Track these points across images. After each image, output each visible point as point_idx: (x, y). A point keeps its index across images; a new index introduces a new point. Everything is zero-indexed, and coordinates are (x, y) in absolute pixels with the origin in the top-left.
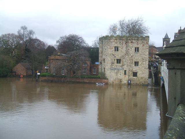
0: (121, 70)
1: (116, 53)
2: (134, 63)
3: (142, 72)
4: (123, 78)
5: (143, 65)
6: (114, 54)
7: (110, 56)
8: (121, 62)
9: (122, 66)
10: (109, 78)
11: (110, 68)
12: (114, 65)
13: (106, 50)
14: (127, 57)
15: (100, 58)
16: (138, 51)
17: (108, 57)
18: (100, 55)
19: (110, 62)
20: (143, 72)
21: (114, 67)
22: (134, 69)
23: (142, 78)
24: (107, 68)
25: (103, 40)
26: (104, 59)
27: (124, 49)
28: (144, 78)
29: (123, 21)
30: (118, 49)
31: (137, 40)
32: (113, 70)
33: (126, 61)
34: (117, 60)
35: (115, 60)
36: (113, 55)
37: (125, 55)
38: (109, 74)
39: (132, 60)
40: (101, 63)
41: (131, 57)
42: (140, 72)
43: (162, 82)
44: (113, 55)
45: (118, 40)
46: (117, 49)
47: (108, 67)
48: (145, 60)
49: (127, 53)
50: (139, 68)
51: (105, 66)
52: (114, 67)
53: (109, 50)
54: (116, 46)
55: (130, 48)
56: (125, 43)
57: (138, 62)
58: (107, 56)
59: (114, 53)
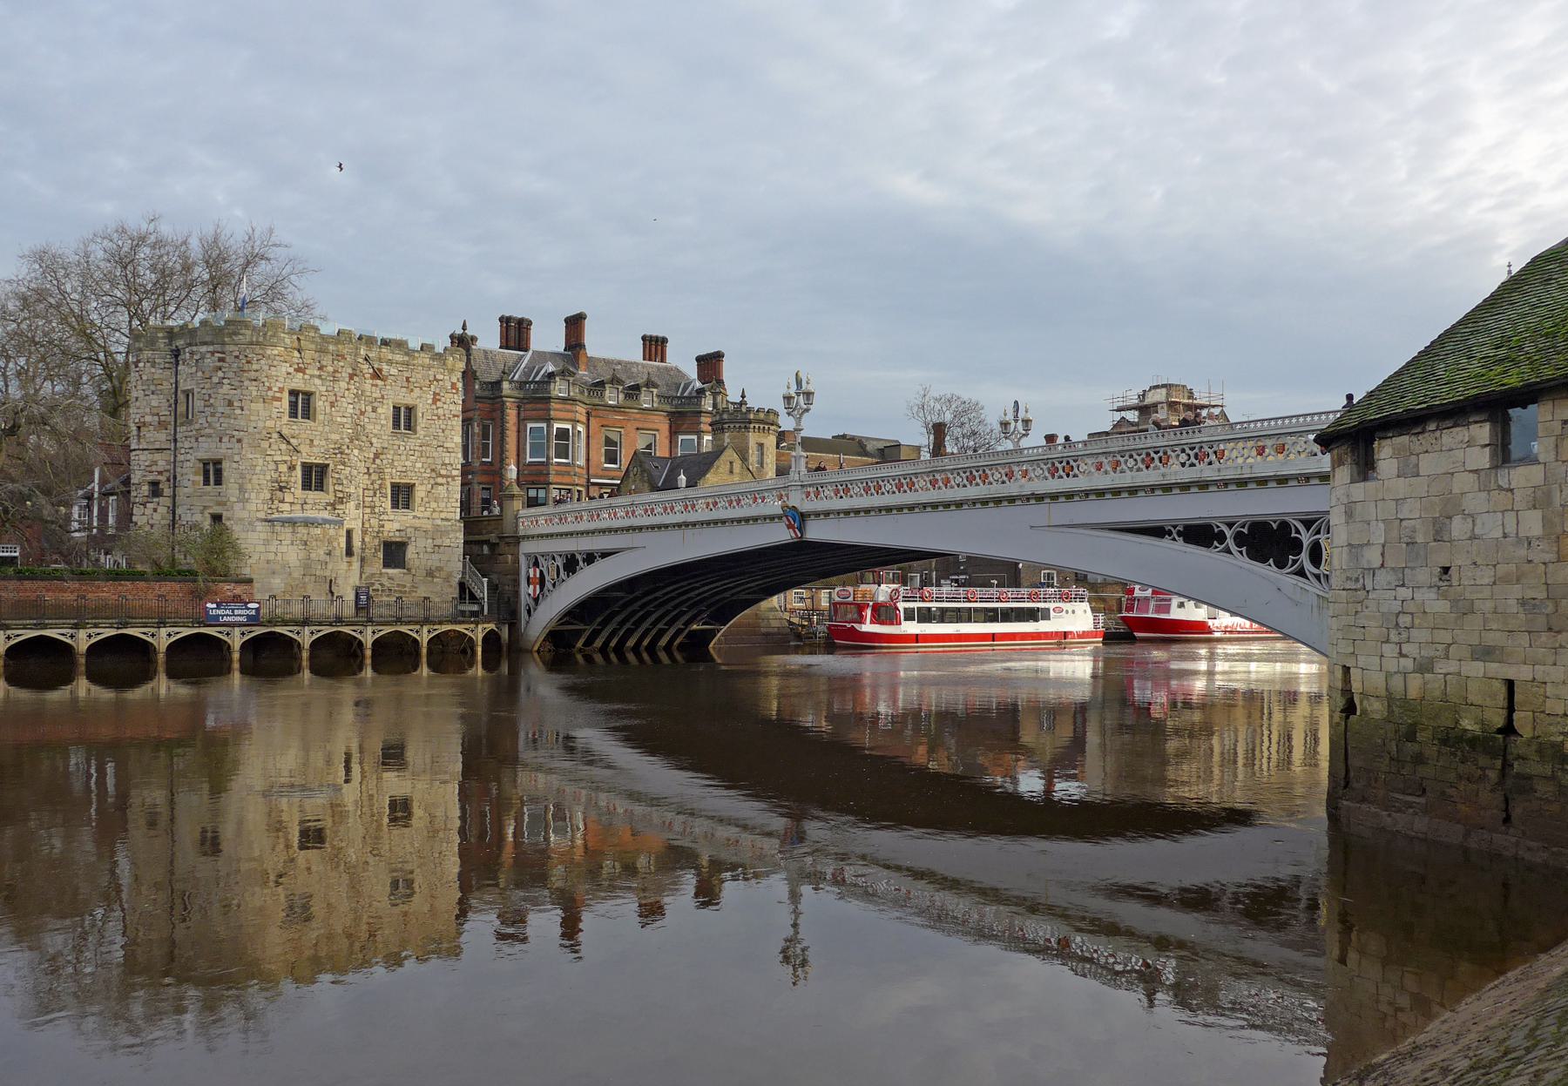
1: (300, 429)
5: (434, 505)
6: (285, 432)
7: (265, 444)
8: (330, 482)
9: (333, 505)
11: (262, 515)
13: (230, 404)
14: (356, 452)
16: (409, 427)
20: (438, 542)
21: (286, 507)
22: (388, 526)
23: (430, 574)
24: (245, 514)
25: (205, 343)
28: (443, 574)
29: (215, 241)
33: (353, 477)
34: (307, 469)
35: (292, 468)
38: (262, 549)
39: (380, 471)
41: (377, 456)
42: (421, 543)
46: (302, 404)
51: (223, 504)
55: (369, 408)
56: (351, 377)
57: (410, 488)
59: (285, 424)
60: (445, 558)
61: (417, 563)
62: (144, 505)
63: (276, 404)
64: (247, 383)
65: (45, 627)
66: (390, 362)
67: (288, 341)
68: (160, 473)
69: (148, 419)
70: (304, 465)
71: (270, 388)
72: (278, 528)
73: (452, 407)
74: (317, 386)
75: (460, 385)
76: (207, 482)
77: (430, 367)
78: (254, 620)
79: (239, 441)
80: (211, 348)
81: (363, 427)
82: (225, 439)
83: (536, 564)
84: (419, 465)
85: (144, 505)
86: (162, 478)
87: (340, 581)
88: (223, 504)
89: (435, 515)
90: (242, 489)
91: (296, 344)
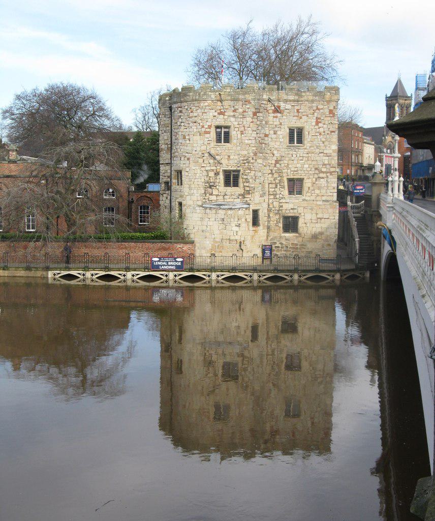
0: (239, 209)
2: (286, 184)
3: (314, 217)
5: (317, 191)
6: (213, 152)
7: (201, 161)
8: (241, 180)
9: (243, 196)
10: (196, 240)
12: (215, 192)
13: (184, 138)
14: (260, 161)
15: (162, 168)
16: (300, 141)
17: (193, 166)
18: (164, 157)
20: (320, 216)
21: (213, 198)
22: (285, 206)
23: (315, 237)
25: (175, 103)
26: (179, 173)
27: (251, 134)
28: (323, 237)
29: (244, 34)
30: (227, 135)
31: (294, 101)
34: (227, 174)
35: (217, 174)
36: (210, 155)
37: (255, 154)
38: (199, 223)
39: (280, 172)
40: (168, 186)
41: (277, 162)
43: (386, 249)
44: (210, 155)
45: (225, 103)
46: (223, 135)
47: (195, 198)
48: (326, 172)
49: (261, 147)
50: (304, 200)
51: (182, 196)
52: (213, 198)
53: (198, 137)
54: (222, 123)
55: (272, 132)
56: (255, 114)
57: (301, 181)
58: (188, 159)
59: (214, 147)
60: (325, 226)
61: (305, 229)
63: (207, 135)
64: (191, 124)
65: (69, 269)
66: (286, 101)
67: (213, 96)
68: (168, 177)
69: (163, 147)
71: (203, 127)
73: (331, 126)
74: (232, 122)
76: (178, 185)
77: (313, 101)
78: (179, 268)
82: (182, 159)
84: (306, 166)
86: (169, 180)
87: (248, 243)
89: (318, 198)
90: (190, 188)
91: (218, 98)
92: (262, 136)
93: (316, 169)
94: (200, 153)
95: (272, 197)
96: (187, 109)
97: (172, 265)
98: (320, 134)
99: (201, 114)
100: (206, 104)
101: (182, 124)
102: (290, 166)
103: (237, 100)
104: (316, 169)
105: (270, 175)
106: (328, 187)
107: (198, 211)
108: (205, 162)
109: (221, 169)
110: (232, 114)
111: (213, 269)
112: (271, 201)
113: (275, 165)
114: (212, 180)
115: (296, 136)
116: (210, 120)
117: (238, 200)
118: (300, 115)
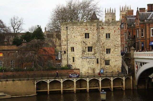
3: (114, 60)
4: (96, 67)
5: (115, 52)
6: (84, 41)
7: (81, 44)
8: (93, 50)
9: (94, 54)
10: (80, 68)
13: (75, 37)
14: (98, 44)
16: (109, 37)
19: (81, 50)
20: (116, 60)
21: (85, 55)
22: (106, 57)
23: (115, 66)
25: (70, 26)
27: (96, 35)
28: (118, 66)
32: (84, 58)
35: (86, 48)
38: (81, 63)
39: (104, 47)
41: (103, 44)
46: (87, 35)
49: (99, 40)
51: (74, 55)
52: (85, 55)
53: (79, 37)
54: (87, 32)
55: (101, 35)
56: (97, 29)
57: (110, 49)
60: (118, 63)
62: (63, 55)
63: (83, 36)
64: (77, 33)
65: (42, 79)
68: (66, 49)
69: (63, 40)
70: (88, 47)
72: (84, 59)
74: (90, 32)
75: (120, 28)
76: (72, 51)
79: (76, 43)
80: (71, 27)
81: (100, 39)
82: (74, 43)
83: (137, 64)
84: (111, 45)
85: (63, 55)
86: (66, 50)
88: (74, 55)
90: (77, 52)
92: (99, 36)
93: (115, 46)
94: (81, 42)
95: (102, 54)
96: (75, 28)
97: (75, 76)
98: (116, 35)
99: (80, 30)
100: (82, 26)
101: (74, 33)
102: (107, 45)
103: (92, 25)
104: (115, 46)
105: (101, 48)
106: (118, 51)
107: (80, 59)
108: (82, 44)
109: (87, 46)
110: (90, 29)
111: (88, 77)
112: (101, 56)
113: (102, 45)
114: (84, 50)
115: (108, 36)
116: (83, 31)
117: (93, 56)
118: (109, 29)
